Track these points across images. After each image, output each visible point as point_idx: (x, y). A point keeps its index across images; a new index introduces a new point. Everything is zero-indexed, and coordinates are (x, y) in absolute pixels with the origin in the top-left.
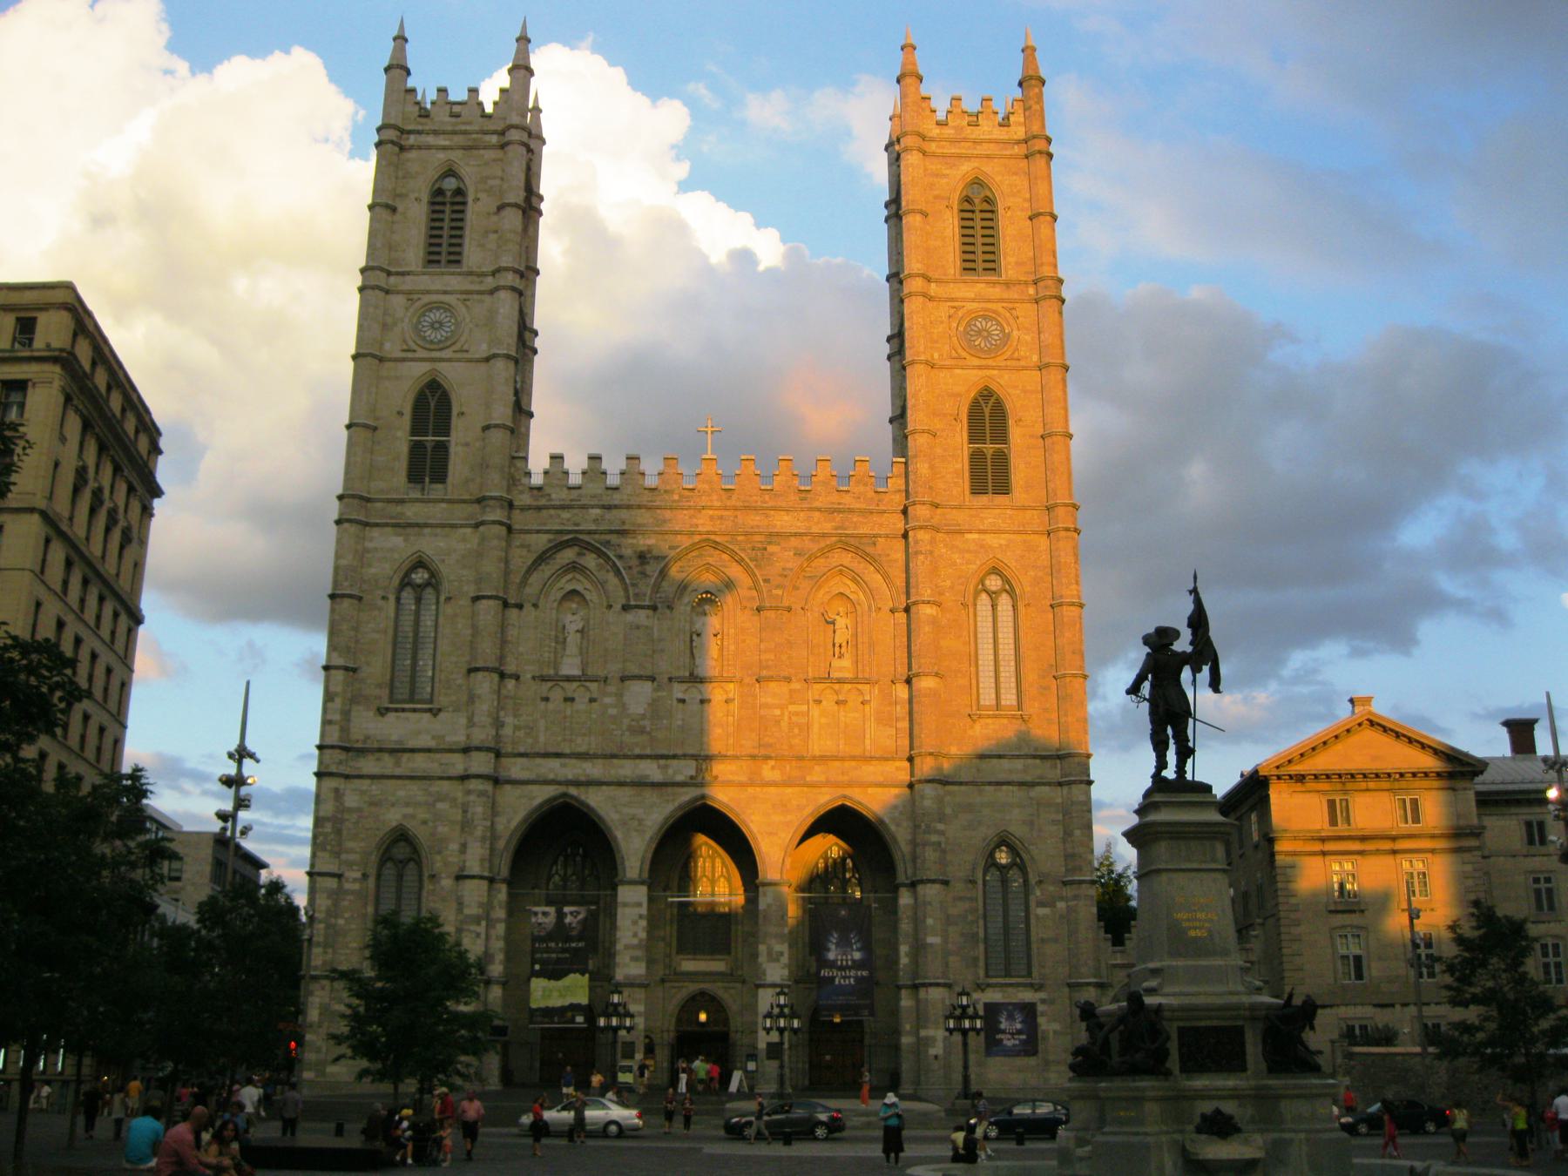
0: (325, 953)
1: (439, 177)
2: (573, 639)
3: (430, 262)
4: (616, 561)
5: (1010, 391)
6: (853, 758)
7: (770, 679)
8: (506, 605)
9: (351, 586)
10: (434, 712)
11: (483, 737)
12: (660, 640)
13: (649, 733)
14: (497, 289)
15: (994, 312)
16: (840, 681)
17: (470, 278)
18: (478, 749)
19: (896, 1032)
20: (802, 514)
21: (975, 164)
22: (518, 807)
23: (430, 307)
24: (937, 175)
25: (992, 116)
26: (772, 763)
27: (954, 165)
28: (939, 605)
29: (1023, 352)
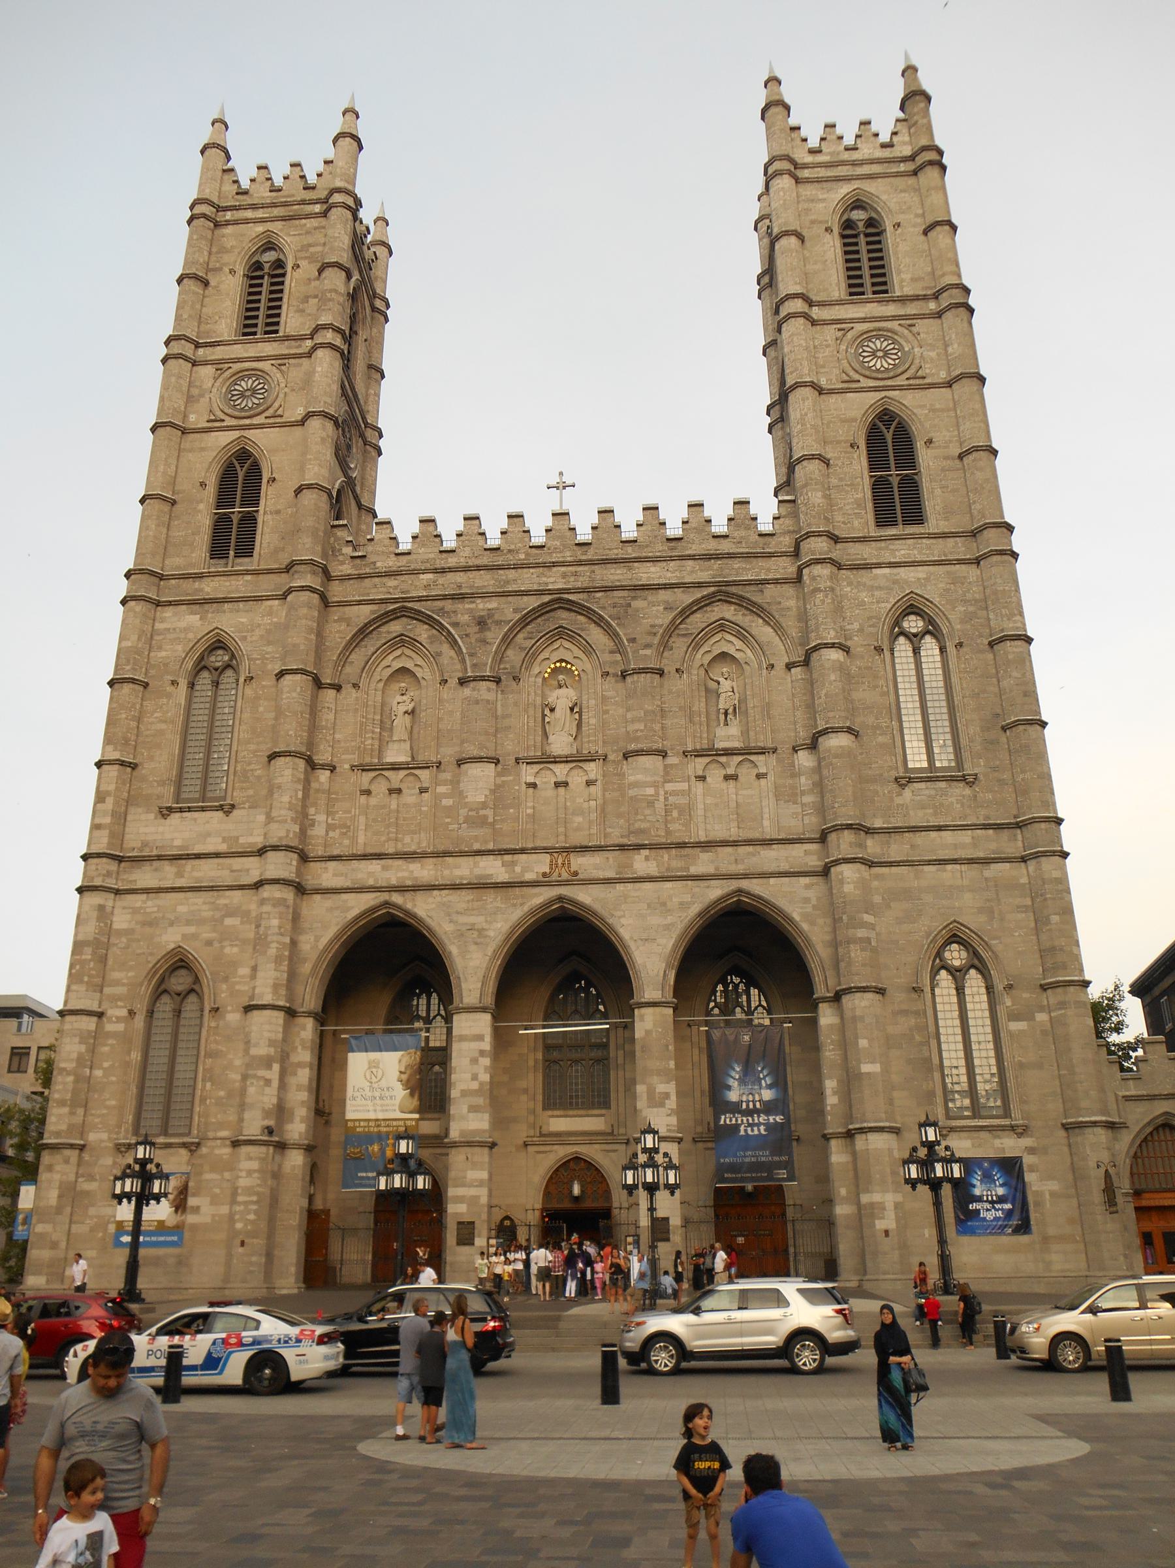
0: (72, 1113)
2: (401, 723)
3: (245, 334)
6: (749, 842)
8: (318, 684)
10: (226, 808)
11: (282, 834)
13: (493, 824)
14: (314, 348)
16: (728, 752)
18: (275, 848)
19: (829, 1202)
20: (672, 564)
21: (856, 184)
23: (241, 375)
24: (812, 201)
25: (873, 138)
26: (645, 852)
28: (846, 650)
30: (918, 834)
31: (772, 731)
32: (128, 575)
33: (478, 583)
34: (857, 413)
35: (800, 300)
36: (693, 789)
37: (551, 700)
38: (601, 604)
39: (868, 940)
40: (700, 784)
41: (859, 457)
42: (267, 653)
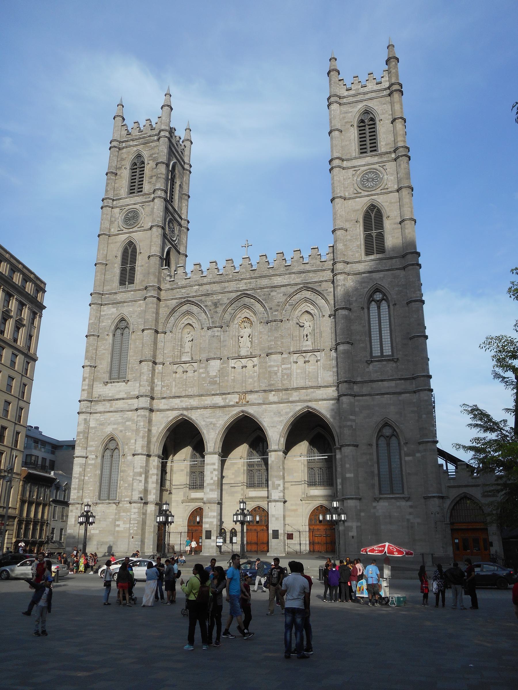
0: (78, 492)
2: (188, 345)
3: (131, 193)
4: (204, 308)
5: (383, 204)
6: (312, 387)
7: (271, 354)
8: (157, 332)
9: (94, 331)
12: (226, 341)
13: (218, 384)
20: (286, 276)
21: (365, 103)
24: (346, 113)
27: (355, 106)
28: (350, 310)
30: (374, 383)
33: (214, 289)
34: (359, 207)
35: (338, 160)
37: (241, 334)
38: (259, 294)
39: (352, 426)
40: (295, 365)
42: (139, 322)
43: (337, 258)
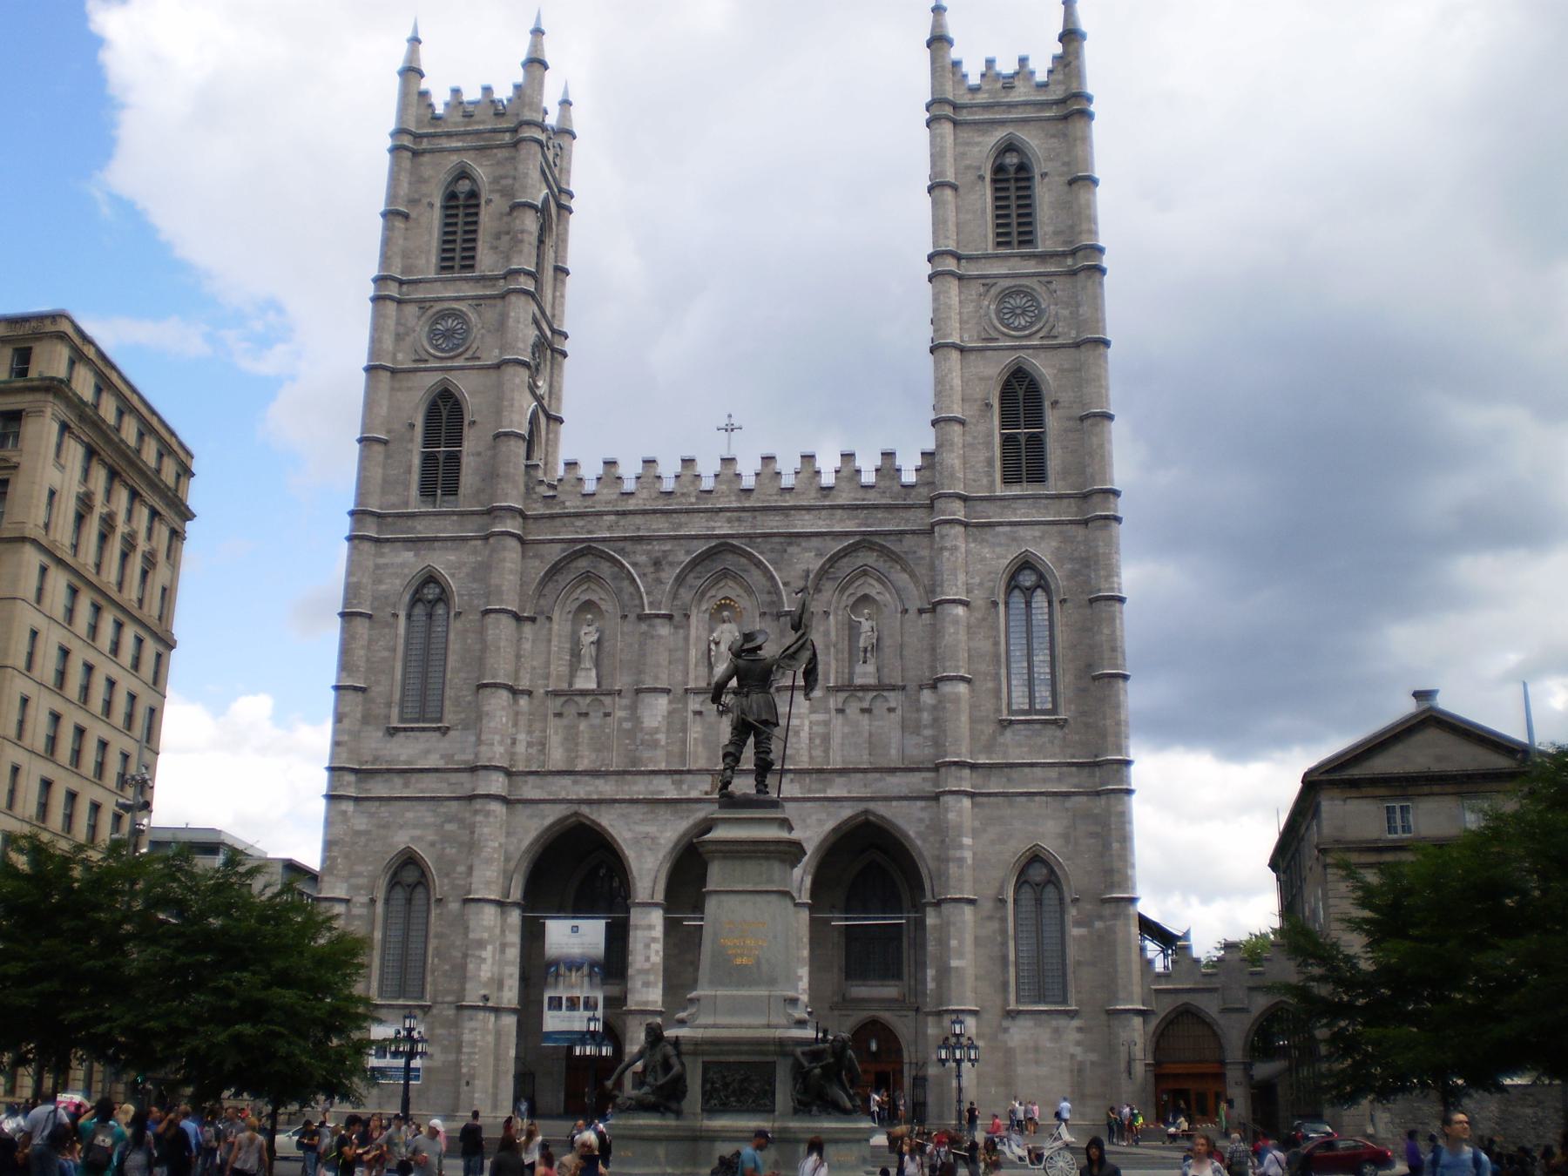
1: (451, 182)
2: (588, 652)
3: (443, 268)
6: (876, 770)
13: (663, 747)
15: (1027, 287)
16: (865, 688)
17: (482, 282)
20: (824, 512)
21: (1010, 129)
22: (532, 828)
24: (968, 144)
28: (965, 604)
29: (1060, 329)
30: (1014, 769)
31: (903, 670)
32: (352, 513)
36: (834, 721)
40: (840, 716)
41: (992, 416)
43: (942, 484)
